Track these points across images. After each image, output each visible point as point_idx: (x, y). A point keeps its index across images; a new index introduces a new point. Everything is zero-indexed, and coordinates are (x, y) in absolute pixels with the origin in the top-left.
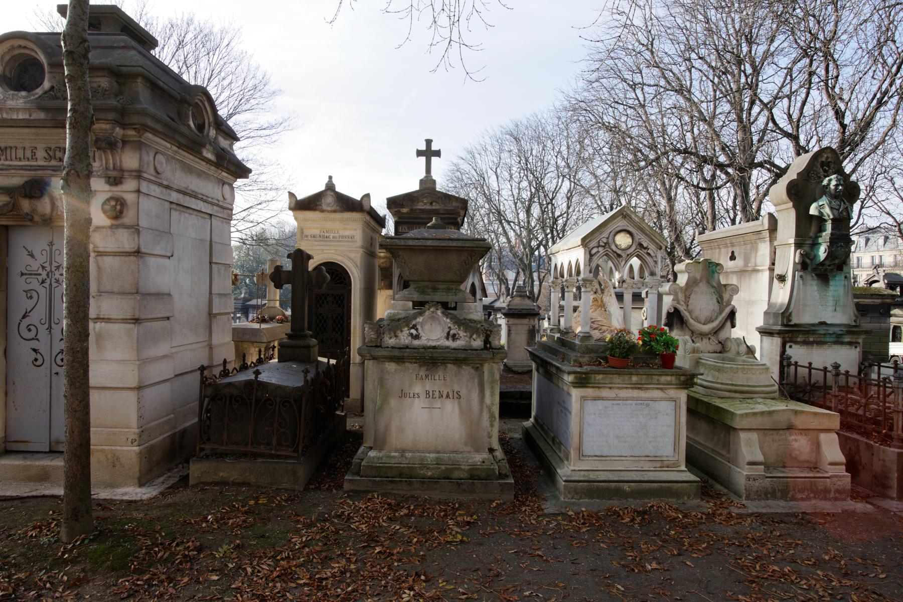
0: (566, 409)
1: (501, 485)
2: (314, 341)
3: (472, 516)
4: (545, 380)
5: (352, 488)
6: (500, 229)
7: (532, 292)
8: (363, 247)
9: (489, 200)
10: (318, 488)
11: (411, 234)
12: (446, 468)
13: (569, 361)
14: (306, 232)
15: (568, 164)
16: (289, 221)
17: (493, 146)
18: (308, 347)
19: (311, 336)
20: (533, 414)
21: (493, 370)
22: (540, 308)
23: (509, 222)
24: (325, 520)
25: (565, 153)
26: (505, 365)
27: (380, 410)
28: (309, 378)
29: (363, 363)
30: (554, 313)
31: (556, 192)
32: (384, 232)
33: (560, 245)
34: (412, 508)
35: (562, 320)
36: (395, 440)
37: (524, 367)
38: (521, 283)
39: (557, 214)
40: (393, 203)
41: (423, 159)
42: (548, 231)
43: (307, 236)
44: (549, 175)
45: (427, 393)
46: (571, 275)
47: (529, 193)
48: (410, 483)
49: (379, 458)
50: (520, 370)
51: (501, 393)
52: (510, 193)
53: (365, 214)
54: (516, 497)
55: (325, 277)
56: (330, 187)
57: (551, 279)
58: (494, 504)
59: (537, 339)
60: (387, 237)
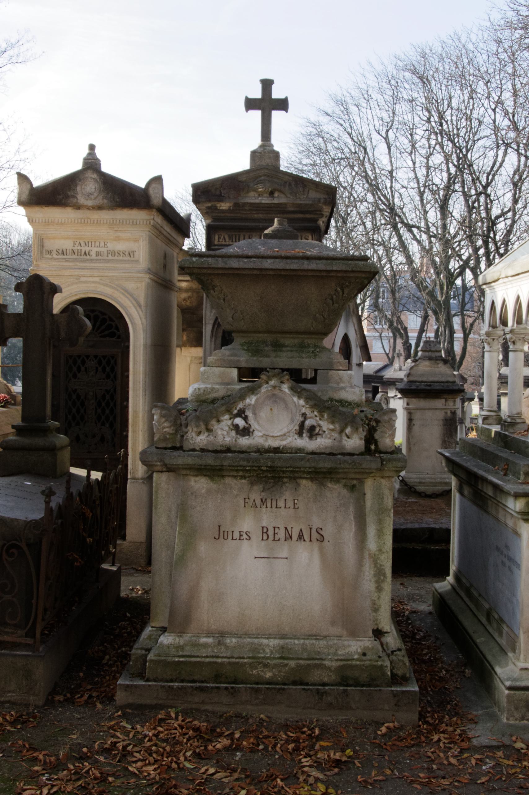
0: (511, 559)
1: (395, 695)
2: (62, 439)
3: (343, 751)
4: (474, 508)
5: (130, 701)
6: (394, 240)
7: (450, 351)
8: (149, 271)
9: (374, 188)
10: (71, 701)
11: (235, 248)
12: (298, 666)
13: (516, 474)
14: (49, 245)
15: (514, 123)
16: (19, 225)
17: (381, 91)
18: (53, 450)
19: (58, 431)
20: (453, 568)
21: (380, 491)
22: (464, 380)
23: (409, 227)
24: (83, 758)
25: (509, 103)
26: (403, 482)
27: (179, 562)
28: (53, 505)
29: (150, 478)
30: (490, 389)
31: (493, 172)
32: (187, 244)
33: (501, 267)
34: (237, 735)
35: (504, 401)
36: (207, 615)
37: (435, 484)
38: (431, 335)
39: (496, 211)
40: (203, 193)
41: (257, 115)
42: (480, 243)
43: (50, 252)
44: (480, 143)
45: (265, 531)
46: (519, 321)
47: (445, 175)
48: (233, 692)
49: (178, 647)
50: (430, 490)
51: (396, 532)
52: (412, 175)
53: (154, 212)
54: (422, 717)
55: (82, 326)
56: (92, 164)
57: (485, 328)
58: (384, 730)
59: (460, 435)
60: (193, 254)
